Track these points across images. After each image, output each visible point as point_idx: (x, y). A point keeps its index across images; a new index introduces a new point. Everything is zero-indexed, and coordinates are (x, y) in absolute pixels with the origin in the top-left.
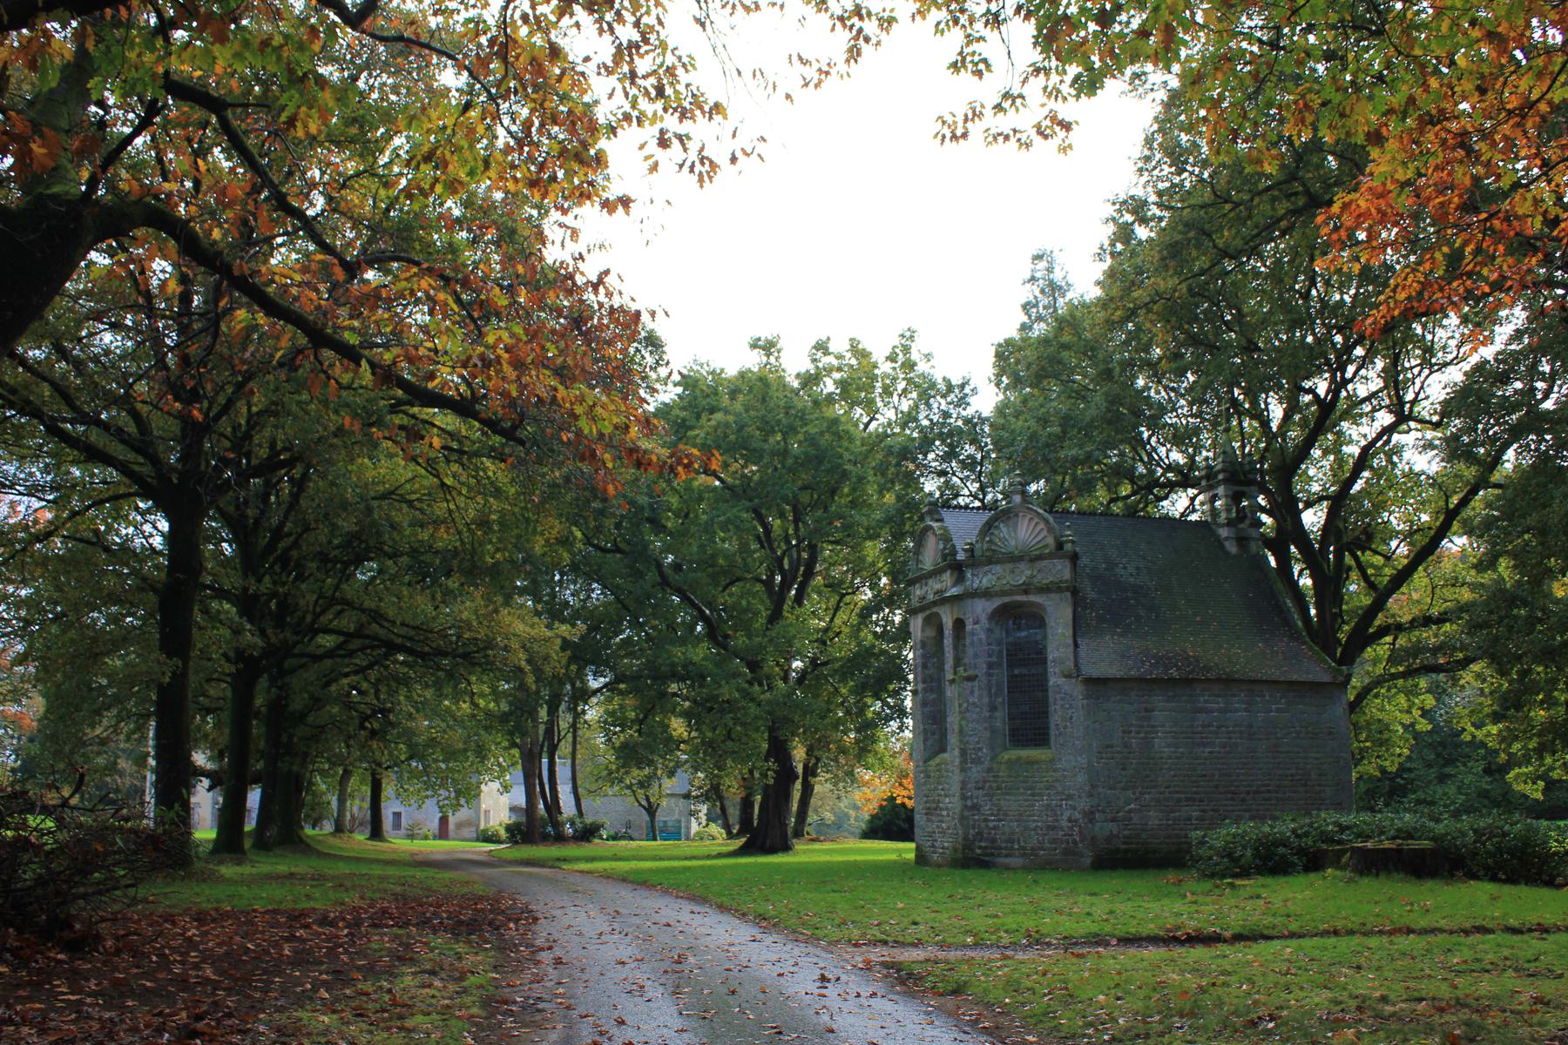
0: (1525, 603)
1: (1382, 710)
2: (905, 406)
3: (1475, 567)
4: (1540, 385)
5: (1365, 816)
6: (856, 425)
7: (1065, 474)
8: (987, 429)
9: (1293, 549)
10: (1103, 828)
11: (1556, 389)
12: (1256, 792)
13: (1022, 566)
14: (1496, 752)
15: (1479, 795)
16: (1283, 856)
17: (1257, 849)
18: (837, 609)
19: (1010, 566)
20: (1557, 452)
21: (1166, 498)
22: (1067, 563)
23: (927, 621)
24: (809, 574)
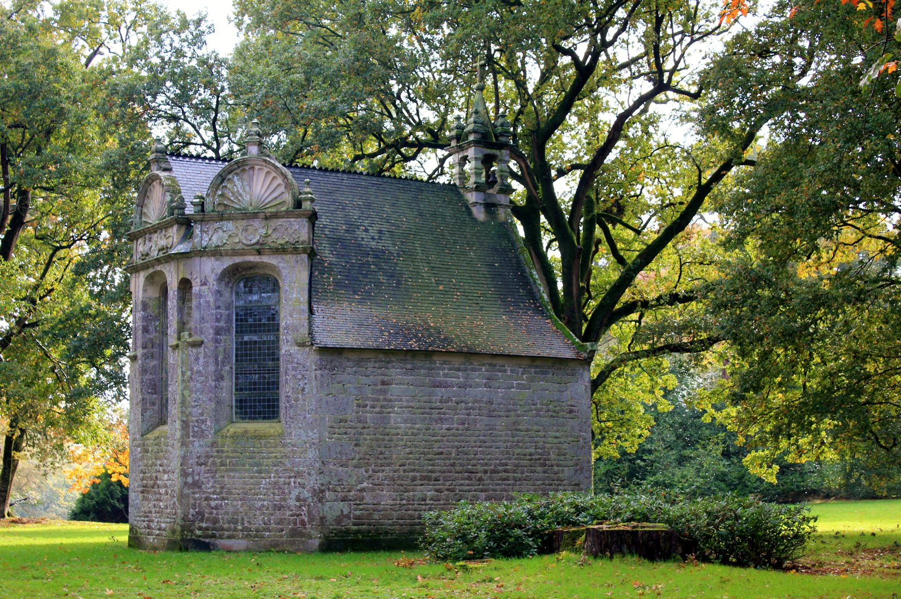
0: (770, 284)
1: (625, 389)
2: (134, 40)
3: (723, 244)
4: (798, 61)
5: (604, 498)
6: (77, 58)
7: (306, 126)
8: (225, 72)
9: (543, 218)
10: (333, 509)
11: (813, 66)
12: (493, 472)
13: (257, 223)
14: (734, 435)
15: (716, 478)
16: (517, 538)
17: (491, 531)
18: (49, 264)
19: (244, 223)
20: (809, 131)
21: (414, 158)
22: (305, 223)
23: (150, 279)
24: (18, 223)
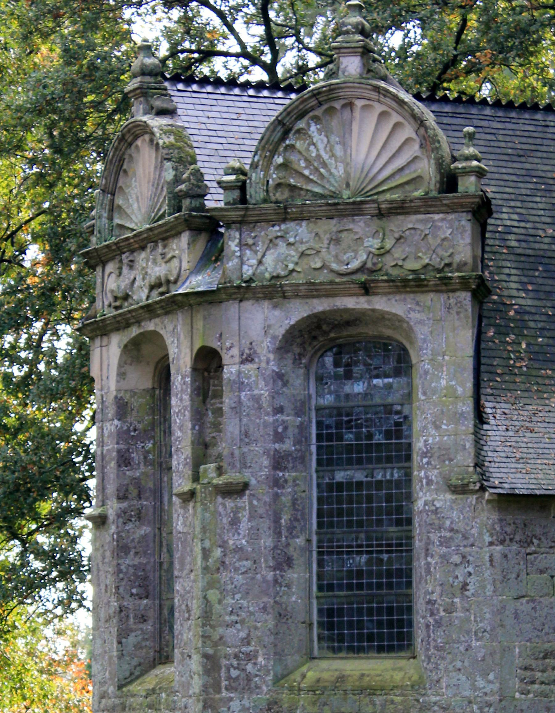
19: (333, 225)
